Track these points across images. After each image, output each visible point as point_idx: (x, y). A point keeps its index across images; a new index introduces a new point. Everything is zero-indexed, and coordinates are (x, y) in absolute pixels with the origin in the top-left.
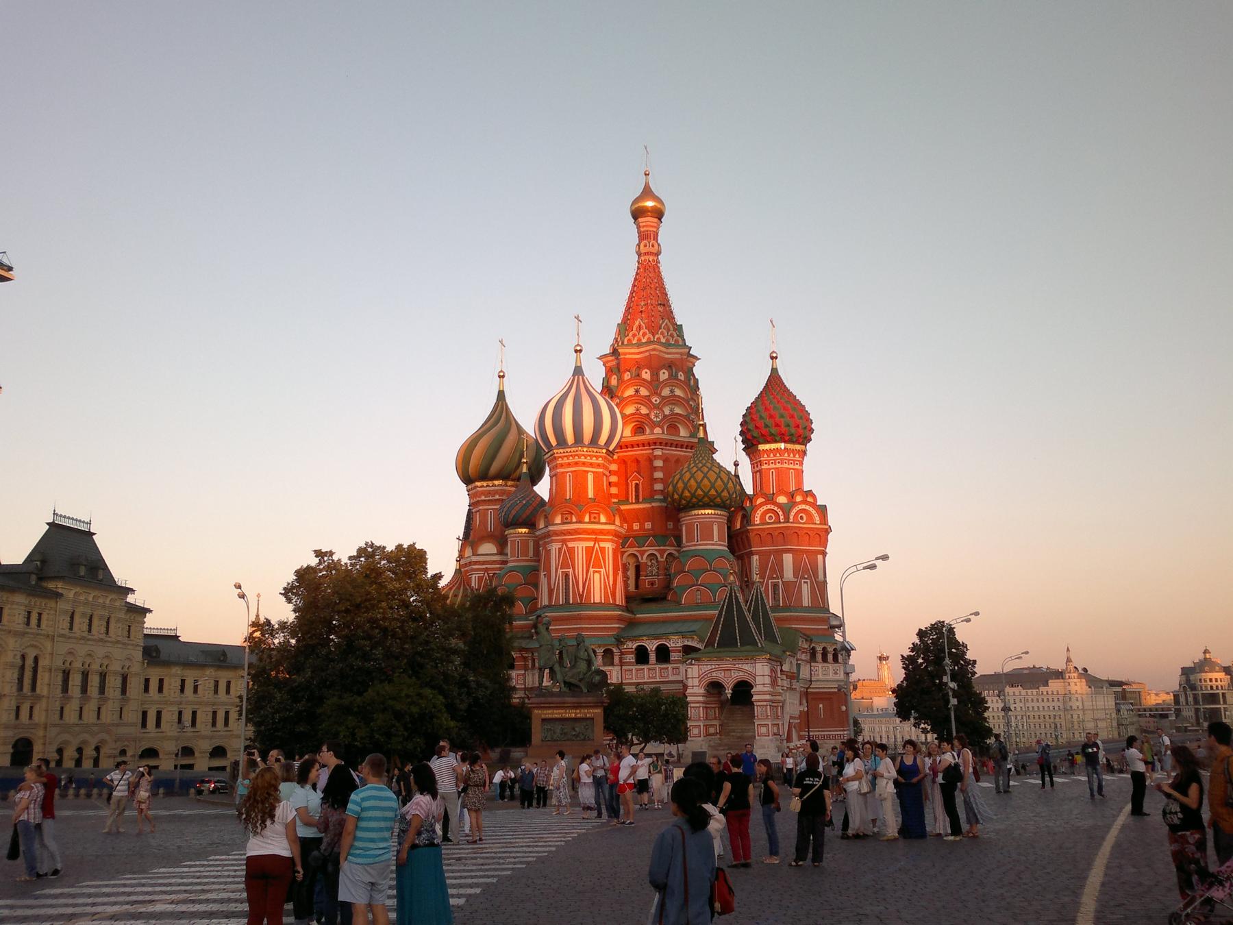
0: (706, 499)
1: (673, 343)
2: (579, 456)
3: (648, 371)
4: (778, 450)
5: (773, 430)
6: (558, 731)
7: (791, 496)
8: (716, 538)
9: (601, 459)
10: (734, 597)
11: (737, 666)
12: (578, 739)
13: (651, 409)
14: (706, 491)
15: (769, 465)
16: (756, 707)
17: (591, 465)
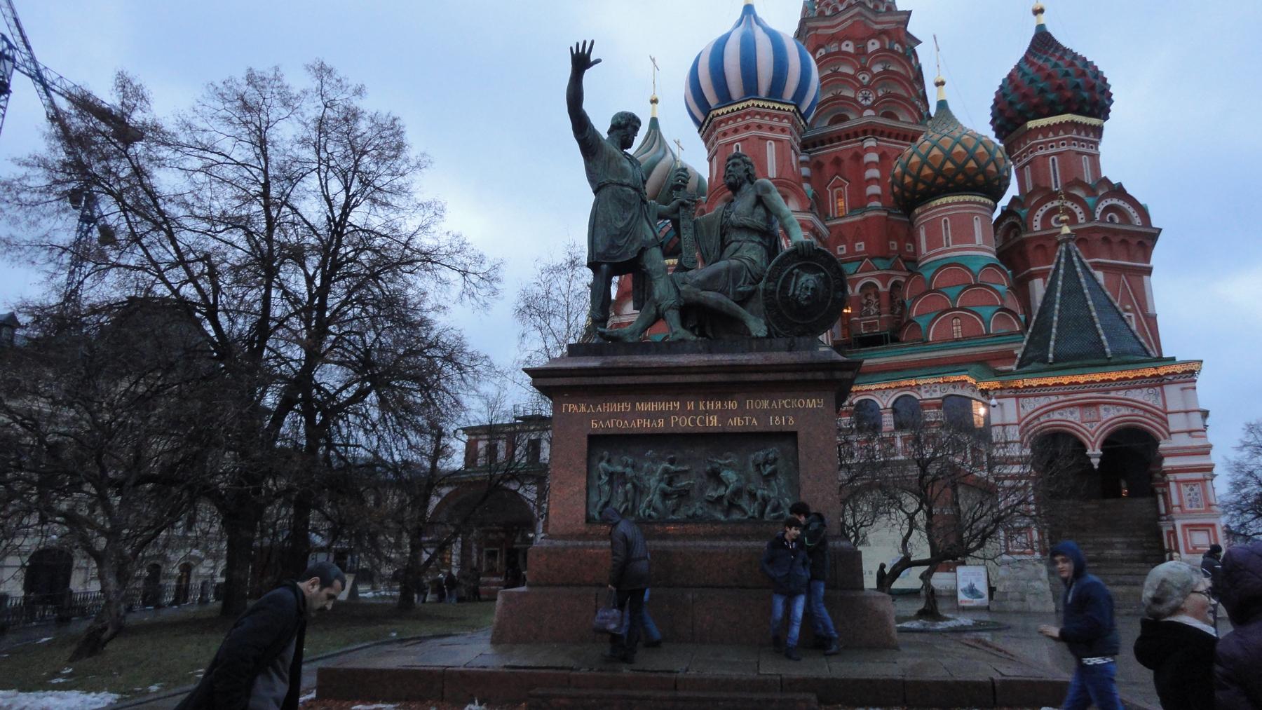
0: (960, 177)
1: (884, 10)
2: (753, 114)
3: (851, 44)
4: (1061, 125)
5: (1052, 96)
6: (653, 482)
7: (1091, 190)
8: (979, 239)
9: (786, 121)
10: (1077, 264)
11: (1113, 394)
12: (736, 516)
13: (857, 90)
14: (960, 161)
15: (1047, 149)
16: (1173, 486)
17: (771, 129)
